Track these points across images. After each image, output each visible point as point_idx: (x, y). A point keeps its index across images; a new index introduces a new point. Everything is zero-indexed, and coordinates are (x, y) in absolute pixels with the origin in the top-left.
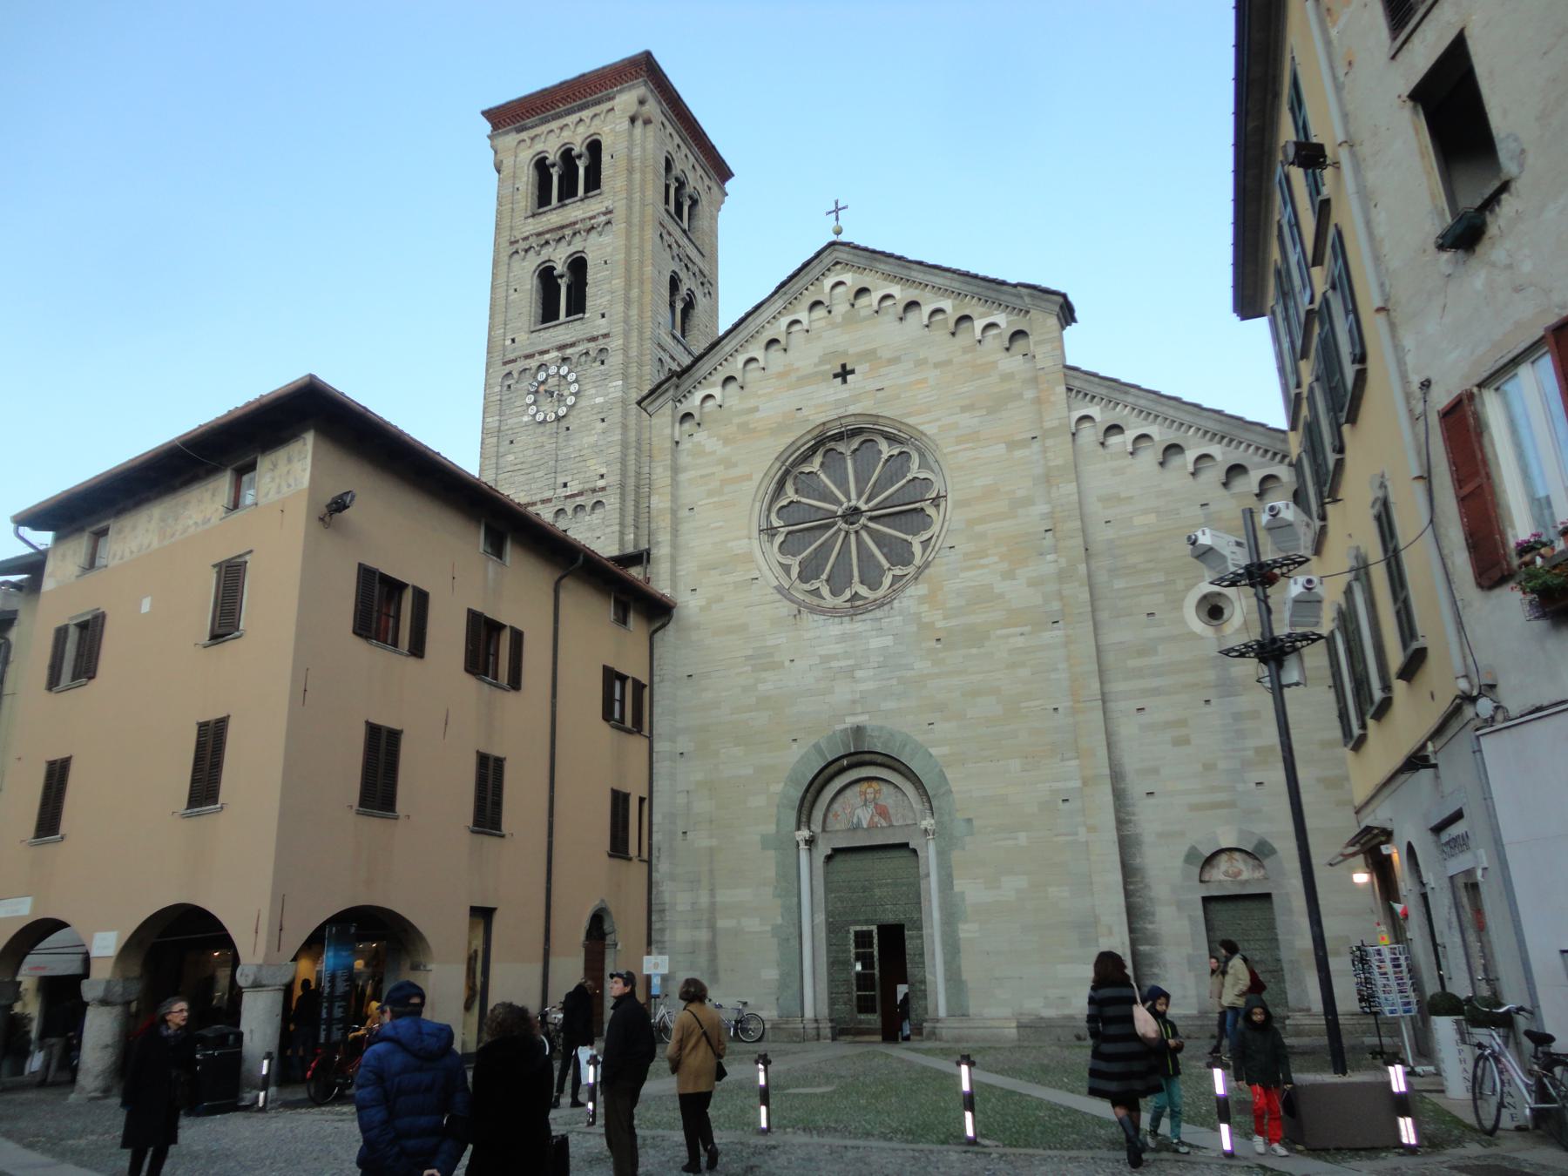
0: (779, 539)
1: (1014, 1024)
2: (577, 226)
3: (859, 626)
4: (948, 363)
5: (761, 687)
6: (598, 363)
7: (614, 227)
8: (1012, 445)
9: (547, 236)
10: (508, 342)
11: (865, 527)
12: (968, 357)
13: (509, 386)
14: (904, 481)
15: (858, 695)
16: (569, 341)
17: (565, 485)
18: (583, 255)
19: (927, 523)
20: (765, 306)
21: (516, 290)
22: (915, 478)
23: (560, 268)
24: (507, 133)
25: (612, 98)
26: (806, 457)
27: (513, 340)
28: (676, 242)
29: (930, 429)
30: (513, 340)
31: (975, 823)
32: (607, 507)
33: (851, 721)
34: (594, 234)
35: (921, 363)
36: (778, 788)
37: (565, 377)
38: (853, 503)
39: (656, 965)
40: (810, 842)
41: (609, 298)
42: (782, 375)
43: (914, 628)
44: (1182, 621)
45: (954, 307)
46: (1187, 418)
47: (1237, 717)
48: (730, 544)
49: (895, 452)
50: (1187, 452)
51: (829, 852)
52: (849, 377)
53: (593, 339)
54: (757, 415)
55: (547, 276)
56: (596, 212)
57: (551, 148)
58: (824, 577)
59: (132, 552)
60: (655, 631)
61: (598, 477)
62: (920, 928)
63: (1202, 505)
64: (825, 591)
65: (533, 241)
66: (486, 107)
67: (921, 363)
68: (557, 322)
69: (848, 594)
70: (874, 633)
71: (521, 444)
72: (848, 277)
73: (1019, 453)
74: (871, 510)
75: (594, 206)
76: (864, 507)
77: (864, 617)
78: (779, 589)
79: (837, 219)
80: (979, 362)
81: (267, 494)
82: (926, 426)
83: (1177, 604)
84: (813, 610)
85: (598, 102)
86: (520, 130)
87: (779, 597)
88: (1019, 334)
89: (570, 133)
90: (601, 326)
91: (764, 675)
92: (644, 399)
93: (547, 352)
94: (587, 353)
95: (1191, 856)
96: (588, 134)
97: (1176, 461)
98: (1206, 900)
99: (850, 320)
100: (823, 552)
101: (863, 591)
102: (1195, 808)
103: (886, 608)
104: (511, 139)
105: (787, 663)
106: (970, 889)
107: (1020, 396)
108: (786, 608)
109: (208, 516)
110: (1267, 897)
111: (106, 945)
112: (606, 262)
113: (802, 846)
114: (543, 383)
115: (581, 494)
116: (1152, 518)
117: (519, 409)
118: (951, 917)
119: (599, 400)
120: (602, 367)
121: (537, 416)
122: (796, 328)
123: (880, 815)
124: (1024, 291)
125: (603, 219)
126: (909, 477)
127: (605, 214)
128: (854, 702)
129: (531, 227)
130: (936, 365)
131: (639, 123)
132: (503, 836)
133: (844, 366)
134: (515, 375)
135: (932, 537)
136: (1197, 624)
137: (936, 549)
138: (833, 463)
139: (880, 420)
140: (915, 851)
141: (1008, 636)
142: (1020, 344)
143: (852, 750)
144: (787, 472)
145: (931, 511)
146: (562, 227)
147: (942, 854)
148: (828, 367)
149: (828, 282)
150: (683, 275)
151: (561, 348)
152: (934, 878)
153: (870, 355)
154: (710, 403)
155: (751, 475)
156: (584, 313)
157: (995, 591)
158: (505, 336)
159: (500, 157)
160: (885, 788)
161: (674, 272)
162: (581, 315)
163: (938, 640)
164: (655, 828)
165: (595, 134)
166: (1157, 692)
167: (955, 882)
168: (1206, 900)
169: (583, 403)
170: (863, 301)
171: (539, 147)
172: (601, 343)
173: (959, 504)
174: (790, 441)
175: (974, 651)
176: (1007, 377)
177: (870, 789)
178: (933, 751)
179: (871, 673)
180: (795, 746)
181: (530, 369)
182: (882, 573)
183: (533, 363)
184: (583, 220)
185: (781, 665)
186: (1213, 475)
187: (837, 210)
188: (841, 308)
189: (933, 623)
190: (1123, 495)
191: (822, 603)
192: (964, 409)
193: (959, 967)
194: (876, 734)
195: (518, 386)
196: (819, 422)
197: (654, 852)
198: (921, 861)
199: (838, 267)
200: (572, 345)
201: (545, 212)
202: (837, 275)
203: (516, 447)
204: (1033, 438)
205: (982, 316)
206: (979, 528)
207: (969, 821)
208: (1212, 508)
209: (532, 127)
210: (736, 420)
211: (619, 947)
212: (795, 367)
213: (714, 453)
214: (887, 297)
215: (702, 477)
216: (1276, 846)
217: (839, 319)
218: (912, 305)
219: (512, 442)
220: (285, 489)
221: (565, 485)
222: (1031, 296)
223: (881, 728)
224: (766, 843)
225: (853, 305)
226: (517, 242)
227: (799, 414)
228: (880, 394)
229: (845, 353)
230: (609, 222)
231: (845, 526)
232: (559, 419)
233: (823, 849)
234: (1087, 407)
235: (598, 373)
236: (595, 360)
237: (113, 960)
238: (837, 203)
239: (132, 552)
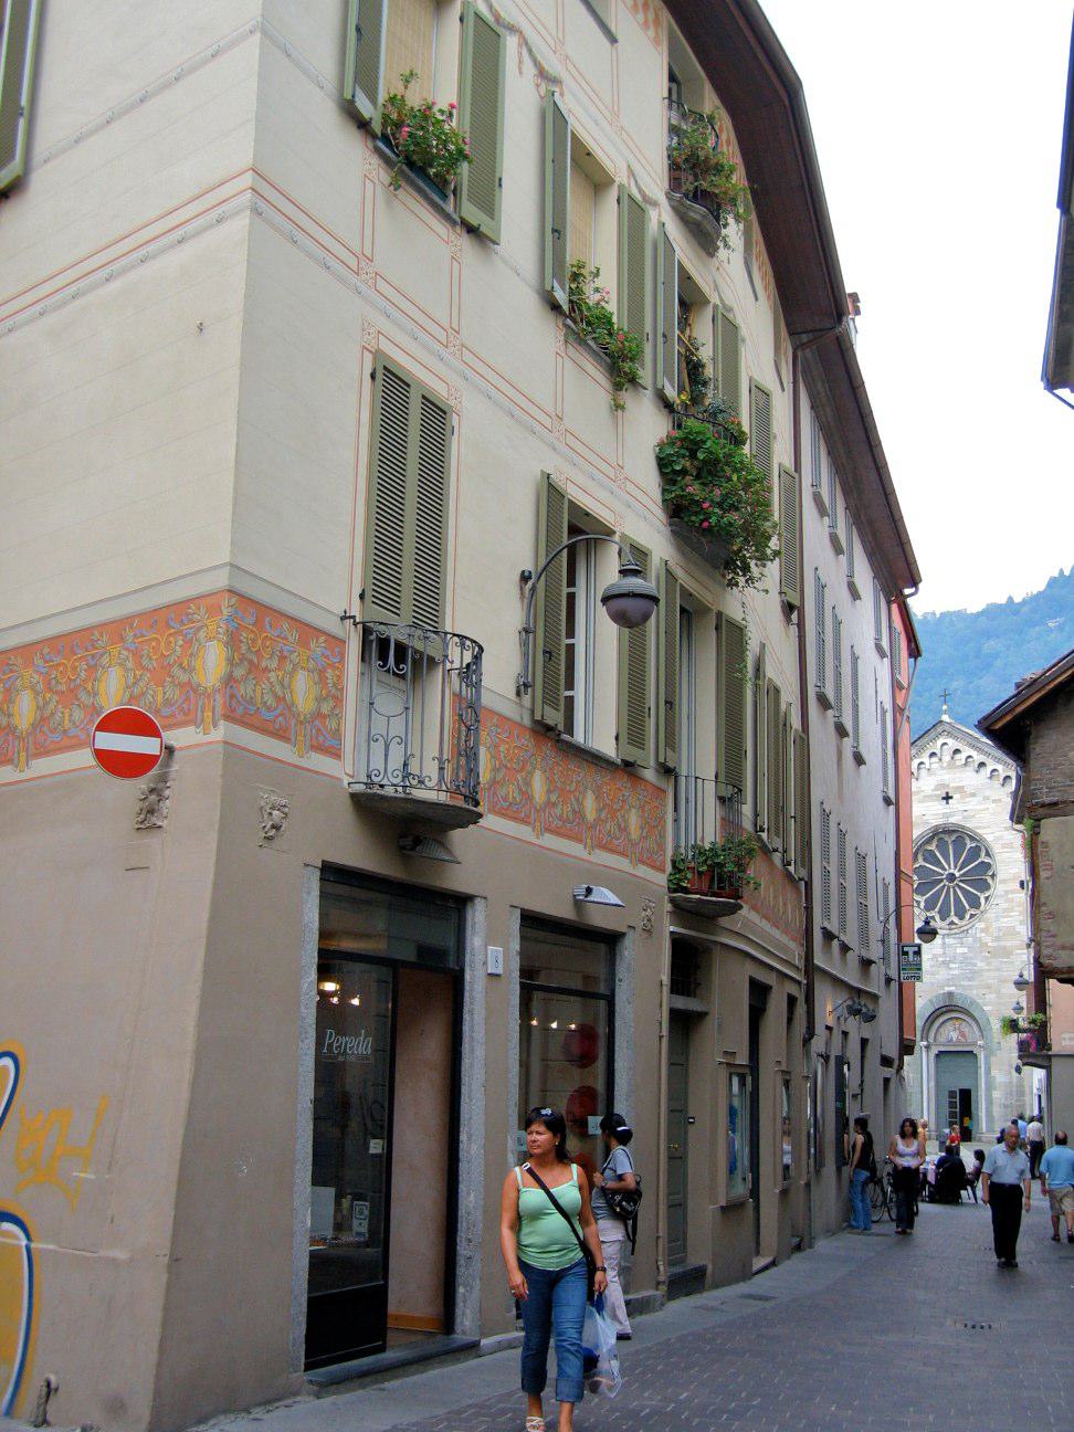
4: (1000, 800)
19: (988, 887)
22: (983, 862)
26: (929, 841)
29: (989, 838)
33: (947, 989)
35: (986, 798)
38: (952, 871)
40: (927, 1047)
49: (974, 845)
52: (950, 801)
67: (986, 798)
72: (950, 741)
76: (957, 874)
99: (952, 766)
100: (936, 896)
101: (956, 920)
118: (989, 1088)
122: (922, 766)
126: (980, 860)
130: (994, 801)
133: (947, 793)
140: (976, 1055)
145: (990, 881)
147: (986, 1057)
152: (983, 1069)
153: (960, 789)
160: (964, 1023)
170: (957, 756)
173: (1004, 881)
178: (985, 1008)
179: (957, 966)
182: (965, 911)
188: (947, 758)
206: (1010, 896)
214: (970, 757)
217: (945, 764)
218: (982, 764)
233: (935, 1051)
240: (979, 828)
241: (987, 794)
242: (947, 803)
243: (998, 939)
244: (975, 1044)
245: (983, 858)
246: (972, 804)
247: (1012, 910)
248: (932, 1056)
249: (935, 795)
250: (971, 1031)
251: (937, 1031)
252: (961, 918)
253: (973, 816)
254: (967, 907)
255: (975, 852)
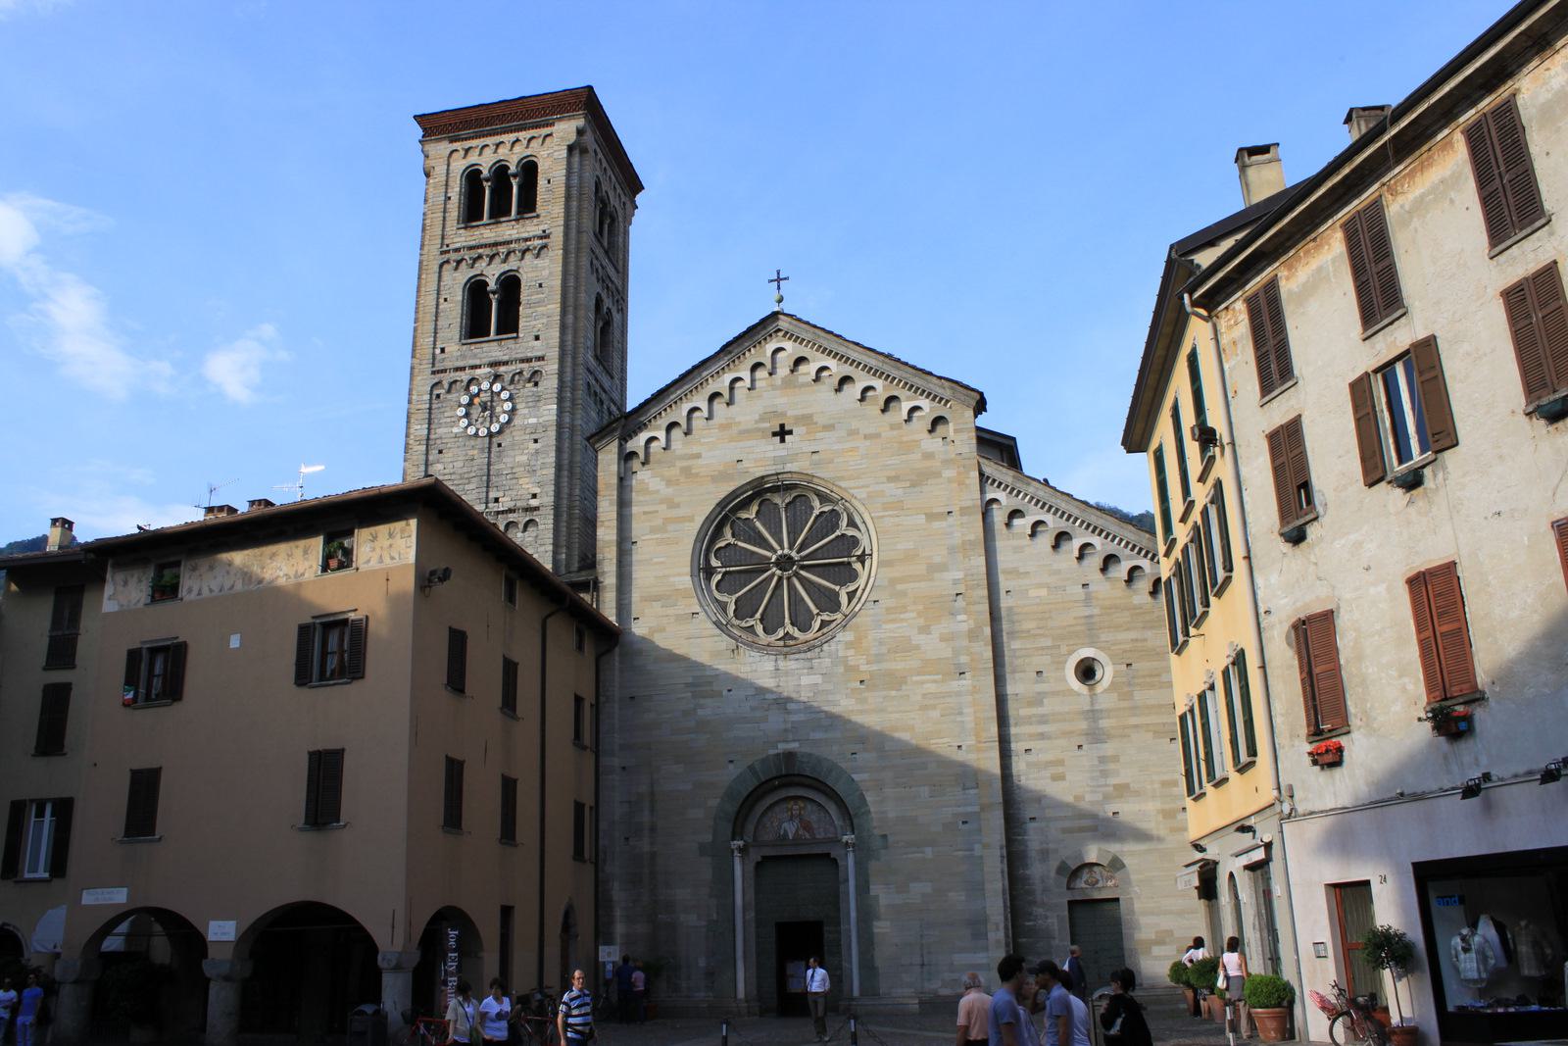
0: (717, 578)
1: (917, 1001)
2: (513, 246)
3: (790, 664)
4: (877, 436)
5: (700, 712)
6: (531, 384)
7: (551, 253)
8: (931, 517)
9: (480, 251)
10: (438, 351)
11: (796, 574)
12: (895, 433)
13: (438, 396)
14: (833, 536)
15: (789, 726)
16: (506, 358)
17: (497, 500)
18: (517, 274)
19: (853, 576)
20: (708, 364)
21: (446, 300)
22: (843, 535)
23: (492, 285)
24: (440, 140)
25: (552, 125)
27: (443, 350)
28: (601, 265)
29: (861, 494)
30: (443, 350)
31: (889, 837)
32: (540, 527)
33: (782, 747)
34: (528, 256)
35: (853, 433)
36: (714, 802)
37: (499, 393)
38: (786, 551)
39: (609, 954)
40: (743, 850)
41: (545, 321)
42: (724, 427)
43: (841, 669)
44: (1064, 679)
45: (884, 386)
46: (1076, 512)
47: (1102, 760)
48: (672, 579)
49: (826, 509)
50: (1074, 540)
51: (759, 859)
52: (787, 437)
53: (528, 360)
54: (700, 462)
55: (476, 290)
56: (531, 234)
57: (486, 162)
58: (758, 615)
59: (211, 591)
60: (603, 654)
61: (538, 496)
62: (838, 924)
63: (1083, 585)
64: (759, 629)
65: (468, 255)
66: (419, 112)
67: (853, 433)
68: (486, 339)
69: (781, 633)
70: (805, 671)
71: (450, 455)
72: (788, 345)
73: (936, 524)
74: (803, 559)
75: (530, 228)
77: (797, 656)
78: (717, 624)
79: (779, 288)
80: (905, 439)
81: (369, 561)
82: (856, 490)
83: (1060, 665)
84: (752, 645)
85: (537, 126)
86: (452, 140)
87: (718, 631)
88: (938, 421)
89: (507, 151)
90: (538, 348)
91: (702, 701)
92: (592, 436)
93: (480, 367)
94: (520, 373)
95: (1062, 869)
96: (525, 155)
97: (1065, 546)
98: (1071, 904)
99: (787, 384)
102: (1065, 831)
103: (817, 650)
104: (443, 148)
105: (725, 693)
106: (883, 895)
107: (938, 475)
108: (725, 642)
109: (301, 571)
110: (1117, 900)
111: (222, 931)
112: (540, 285)
113: (736, 853)
114: (478, 395)
115: (511, 511)
116: (1043, 592)
117: (449, 420)
118: (867, 916)
119: (533, 420)
120: (535, 389)
121: (469, 429)
123: (804, 828)
124: (947, 384)
125: (538, 243)
126: (838, 533)
127: (541, 238)
128: (786, 730)
129: (463, 239)
130: (866, 437)
131: (576, 153)
132: (516, 846)
133: (782, 426)
134: (446, 386)
135: (857, 590)
136: (1075, 684)
137: (863, 600)
138: (768, 515)
139: (815, 480)
140: (835, 860)
141: (923, 683)
142: (940, 429)
143: (784, 772)
144: (725, 519)
145: (857, 566)
146: (496, 244)
148: (767, 425)
149: (771, 347)
150: (604, 296)
151: (491, 365)
152: (852, 883)
153: (806, 419)
154: (654, 444)
155: (693, 516)
156: (518, 333)
157: (913, 642)
158: (435, 344)
159: (431, 163)
160: (809, 807)
161: (598, 293)
162: (515, 335)
163: (861, 682)
164: (601, 835)
165: (531, 156)
166: (1042, 736)
167: (871, 887)
168: (1071, 904)
169: (517, 421)
170: (802, 368)
171: (473, 158)
172: (536, 365)
174: (731, 489)
175: (893, 693)
176: (928, 456)
177: (796, 807)
178: (853, 776)
180: (731, 766)
181: (462, 381)
182: (812, 617)
183: (465, 376)
184: (518, 240)
185: (720, 694)
186: (1094, 561)
187: (779, 280)
188: (783, 371)
189: (858, 666)
190: (1022, 570)
191: (756, 639)
192: (890, 479)
193: (872, 956)
194: (805, 760)
195: (449, 396)
196: (758, 475)
197: (601, 854)
198: (841, 869)
199: (781, 334)
200: (506, 363)
201: (478, 226)
202: (778, 342)
203: (447, 456)
204: (949, 512)
205: (909, 399)
206: (899, 587)
207: (884, 837)
208: (1091, 588)
209: (466, 139)
210: (680, 464)
211: (579, 938)
212: (737, 420)
213: (658, 491)
214: (824, 368)
215: (645, 513)
216: (1125, 862)
217: (779, 382)
218: (845, 380)
219: (440, 452)
220: (387, 560)
221: (497, 500)
222: (952, 388)
223: (810, 755)
224: (703, 849)
225: (792, 371)
226: (448, 252)
227: (740, 465)
228: (815, 456)
229: (784, 414)
230: (544, 247)
231: (779, 572)
232: (490, 435)
233: (755, 856)
234: (995, 492)
235: (530, 394)
236: (529, 381)
237: (232, 946)
238: (778, 273)
239: (211, 591)
240: (842, 478)
241: (855, 424)
242: (783, 440)
243: (879, 658)
244: (836, 841)
245: (843, 528)
246: (826, 442)
247: (904, 609)
248: (751, 867)
249: (763, 430)
250: (824, 821)
251: (758, 822)
252: (804, 628)
253: (831, 462)
254: (815, 611)
255: (830, 520)
